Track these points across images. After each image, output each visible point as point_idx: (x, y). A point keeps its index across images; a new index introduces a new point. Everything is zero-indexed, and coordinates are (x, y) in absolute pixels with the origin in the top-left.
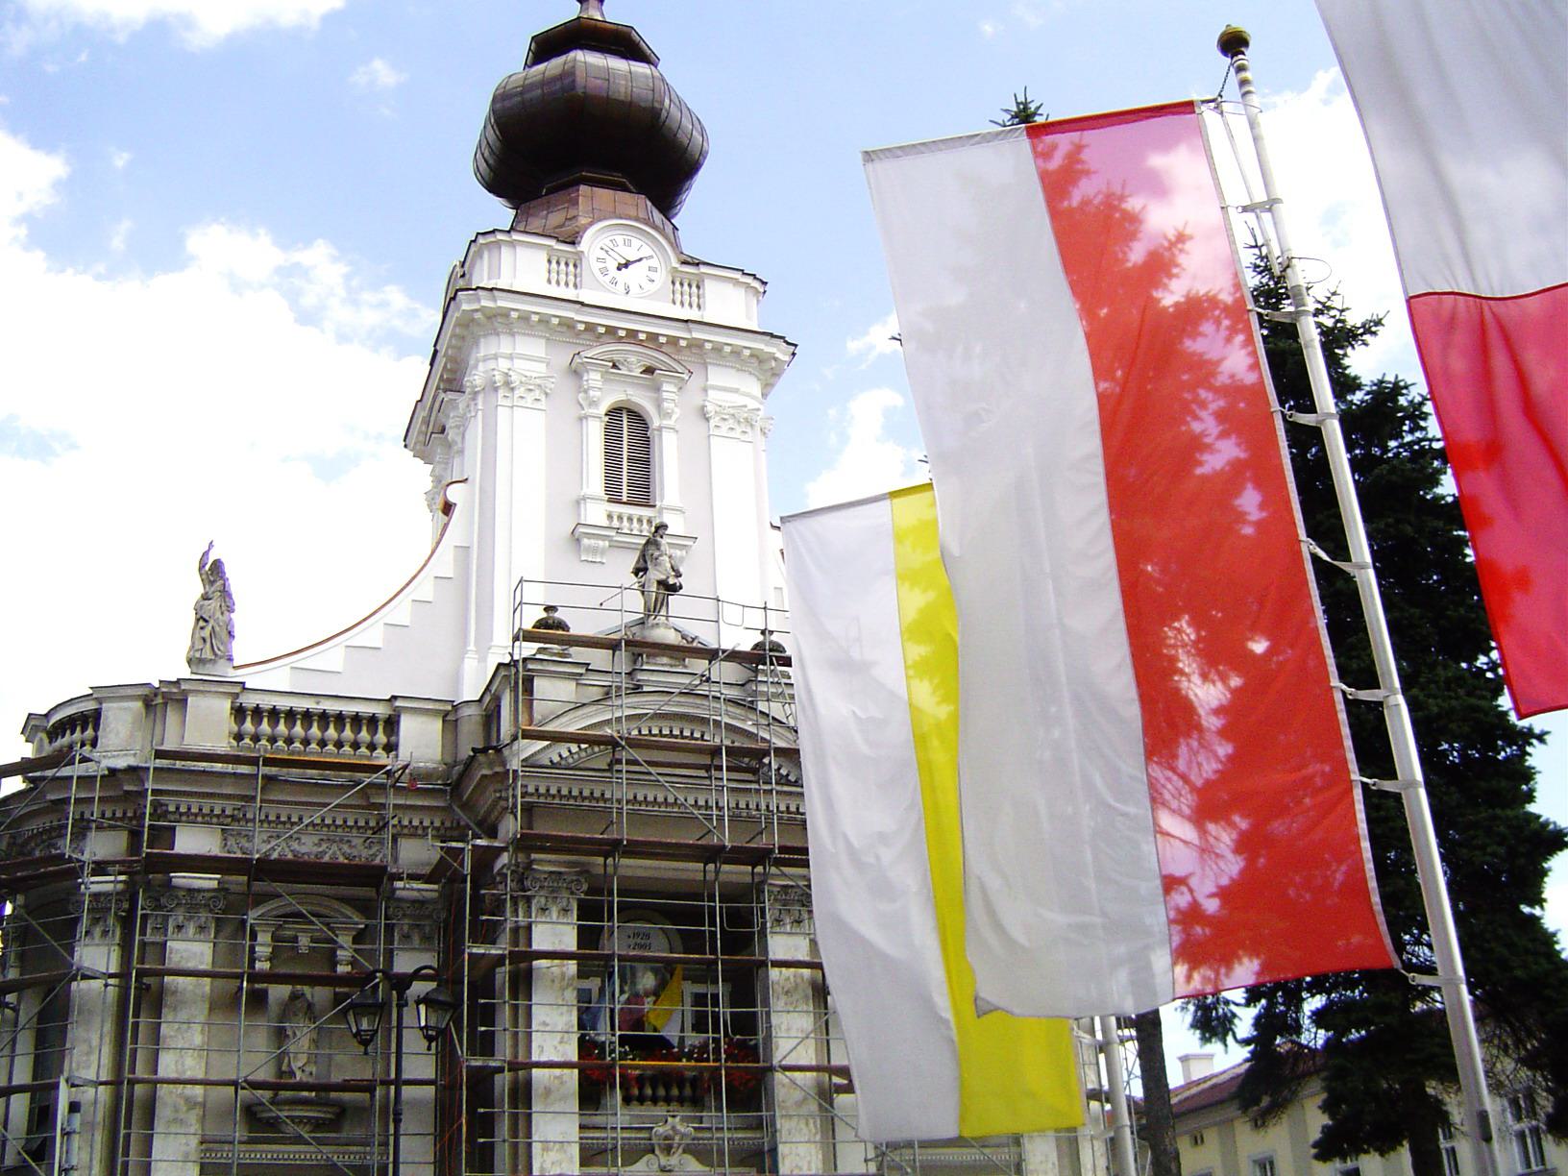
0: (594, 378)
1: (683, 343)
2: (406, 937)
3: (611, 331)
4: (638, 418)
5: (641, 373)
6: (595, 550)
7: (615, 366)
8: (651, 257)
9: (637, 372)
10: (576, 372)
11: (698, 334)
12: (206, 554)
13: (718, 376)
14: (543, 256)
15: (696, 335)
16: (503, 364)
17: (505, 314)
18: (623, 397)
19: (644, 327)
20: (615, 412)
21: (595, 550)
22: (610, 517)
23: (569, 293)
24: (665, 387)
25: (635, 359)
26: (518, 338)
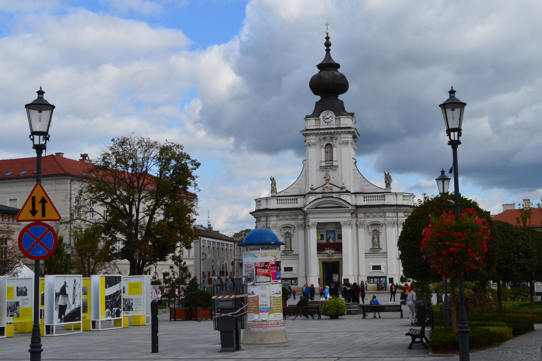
0: (322, 141)
1: (336, 132)
2: (300, 229)
3: (324, 133)
4: (330, 145)
6: (323, 170)
9: (329, 139)
10: (320, 140)
11: (338, 131)
12: (271, 178)
13: (343, 136)
14: (314, 121)
15: (337, 131)
16: (309, 141)
17: (308, 133)
18: (327, 143)
19: (329, 131)
20: (327, 145)
21: (323, 170)
22: (326, 163)
23: (318, 127)
24: (334, 140)
25: (328, 137)
26: (311, 136)
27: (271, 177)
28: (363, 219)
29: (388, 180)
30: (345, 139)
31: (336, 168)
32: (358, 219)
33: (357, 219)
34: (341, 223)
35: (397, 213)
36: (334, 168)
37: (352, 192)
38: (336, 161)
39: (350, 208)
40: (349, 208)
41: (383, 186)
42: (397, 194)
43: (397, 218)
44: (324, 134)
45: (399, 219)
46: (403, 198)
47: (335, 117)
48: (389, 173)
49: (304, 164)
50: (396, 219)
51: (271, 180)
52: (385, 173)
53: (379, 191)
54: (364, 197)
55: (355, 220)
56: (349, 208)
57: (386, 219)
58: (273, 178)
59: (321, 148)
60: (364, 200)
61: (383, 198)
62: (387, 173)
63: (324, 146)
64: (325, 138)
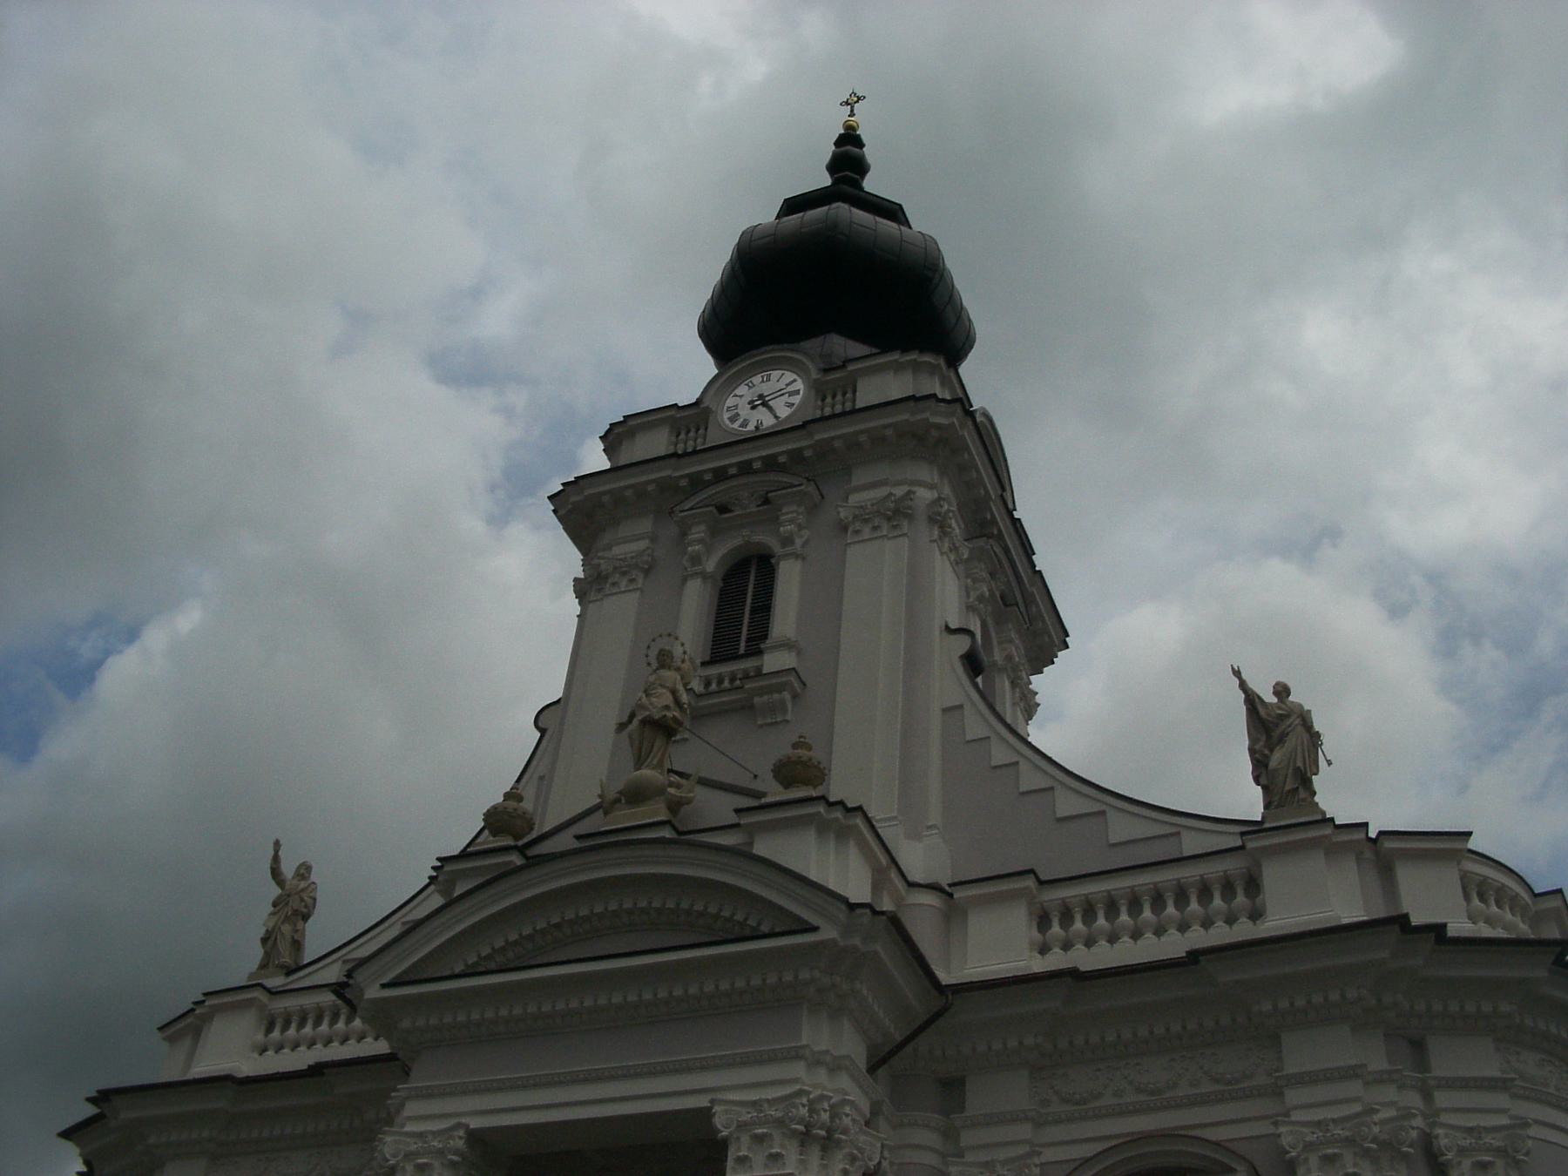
5: (758, 506)
7: (723, 509)
8: (795, 381)
15: (818, 437)
27: (277, 844)
28: (1024, 1131)
29: (1282, 739)
30: (881, 492)
31: (780, 688)
32: (968, 1138)
33: (949, 1134)
34: (718, 1121)
35: (1418, 1047)
36: (762, 691)
37: (916, 876)
38: (787, 645)
39: (828, 933)
40: (815, 929)
41: (1248, 801)
42: (1389, 844)
43: (1427, 1096)
44: (720, 475)
45: (1442, 1099)
46: (1467, 897)
47: (814, 375)
48: (1282, 691)
49: (543, 731)
50: (1414, 1100)
51: (276, 873)
52: (1243, 685)
53: (1192, 844)
54: (1043, 922)
55: (931, 1138)
56: (815, 929)
57: (1294, 1096)
58: (304, 871)
59: (684, 580)
60: (1044, 950)
61: (1241, 899)
62: (1271, 699)
63: (711, 565)
64: (723, 509)
